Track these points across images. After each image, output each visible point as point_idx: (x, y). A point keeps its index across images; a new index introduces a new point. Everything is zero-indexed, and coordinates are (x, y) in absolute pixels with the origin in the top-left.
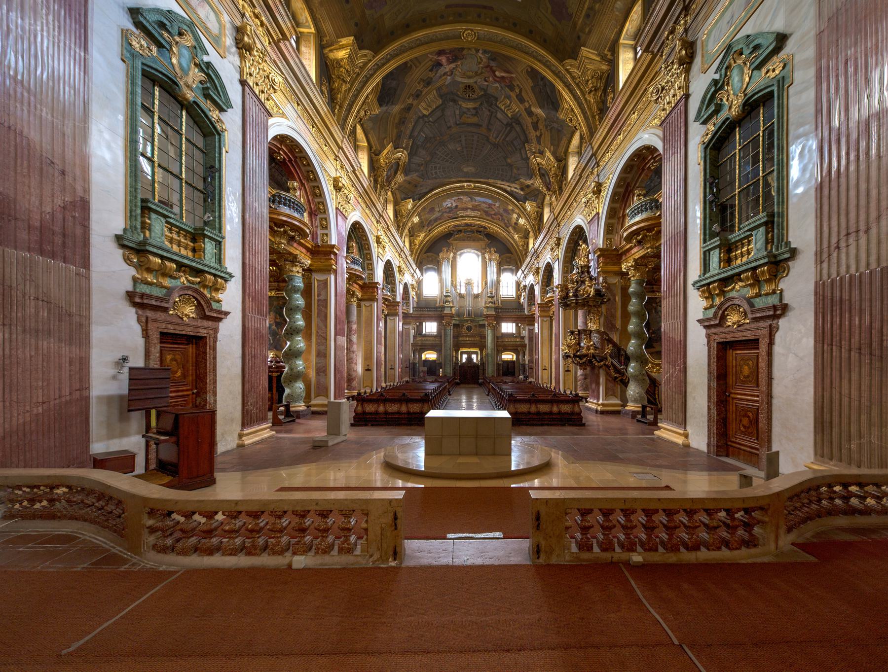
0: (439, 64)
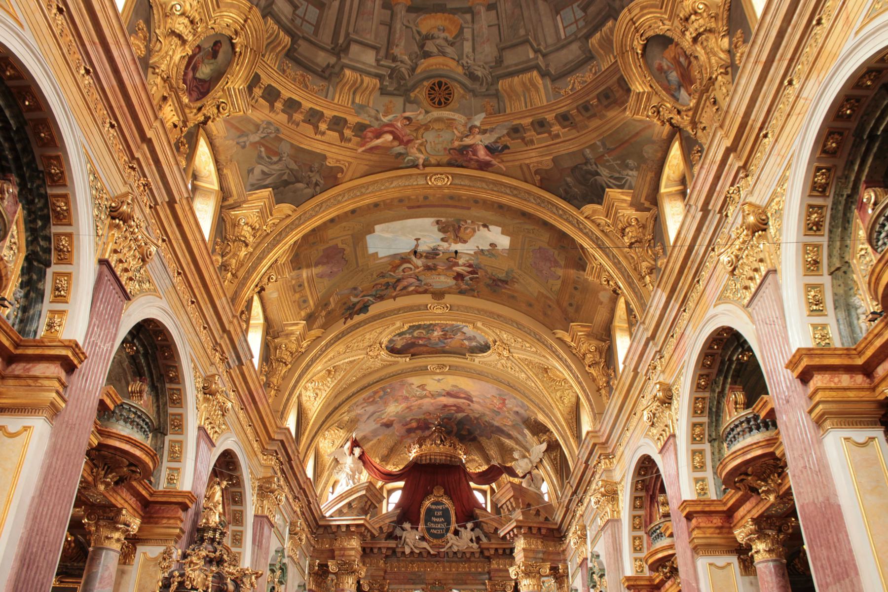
0: (489, 149)
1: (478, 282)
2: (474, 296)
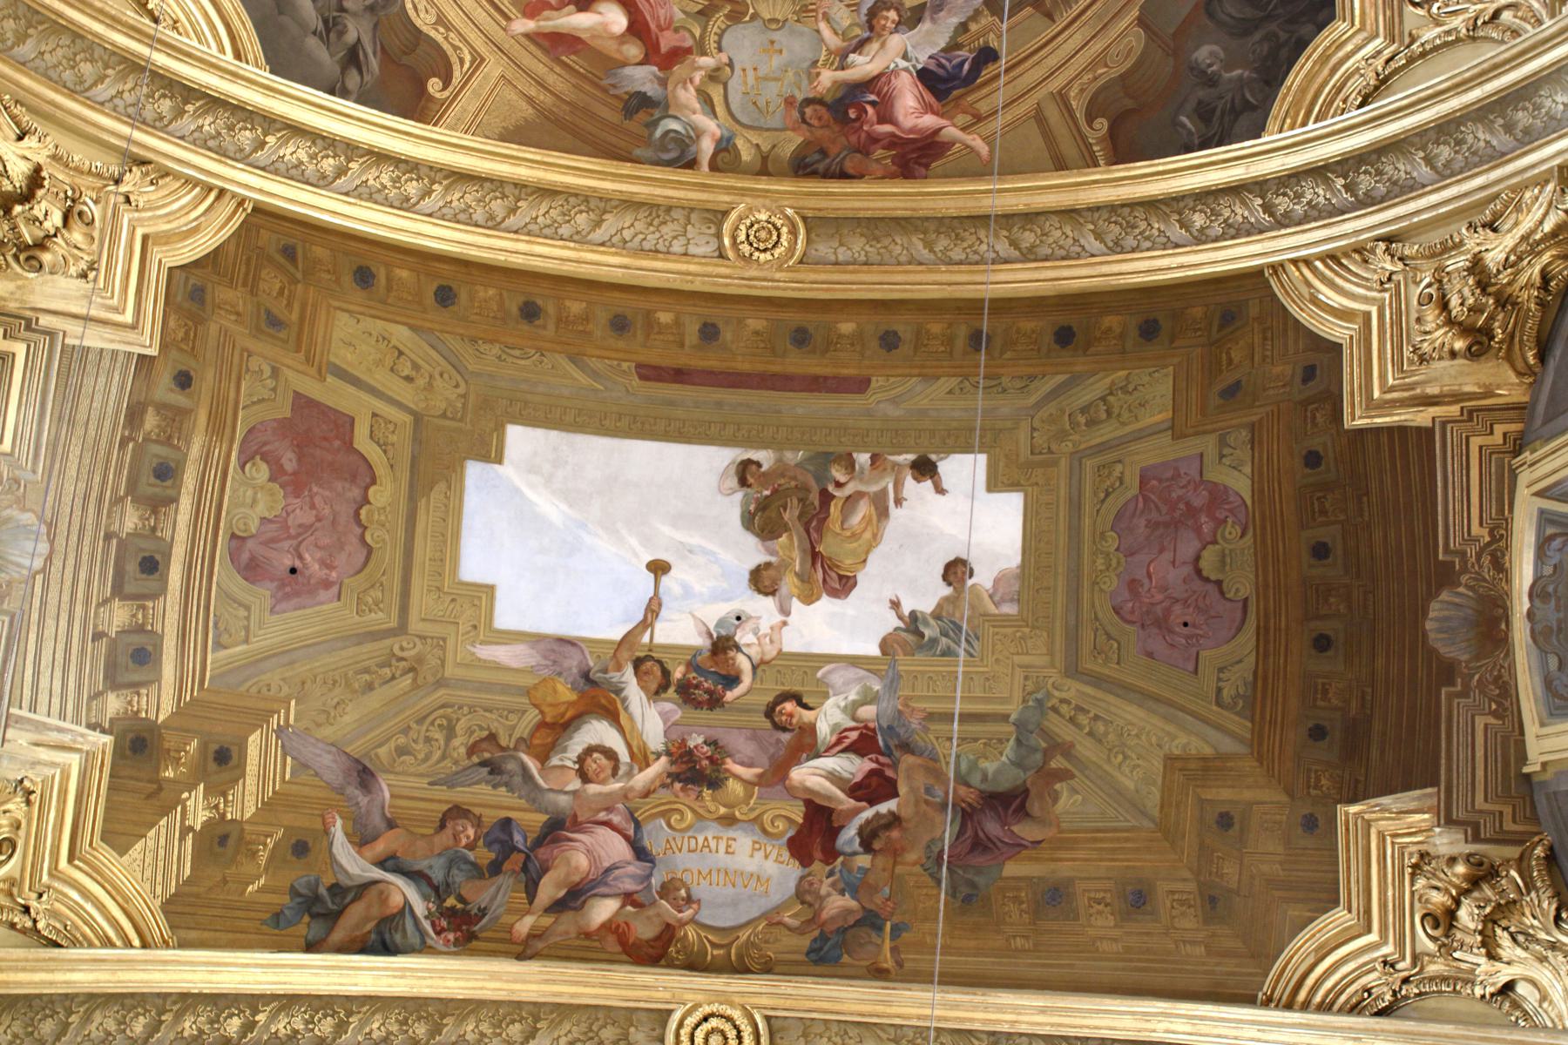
1: (895, 852)
2: (878, 974)
